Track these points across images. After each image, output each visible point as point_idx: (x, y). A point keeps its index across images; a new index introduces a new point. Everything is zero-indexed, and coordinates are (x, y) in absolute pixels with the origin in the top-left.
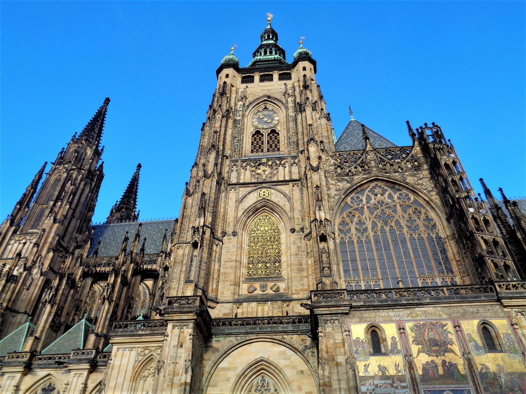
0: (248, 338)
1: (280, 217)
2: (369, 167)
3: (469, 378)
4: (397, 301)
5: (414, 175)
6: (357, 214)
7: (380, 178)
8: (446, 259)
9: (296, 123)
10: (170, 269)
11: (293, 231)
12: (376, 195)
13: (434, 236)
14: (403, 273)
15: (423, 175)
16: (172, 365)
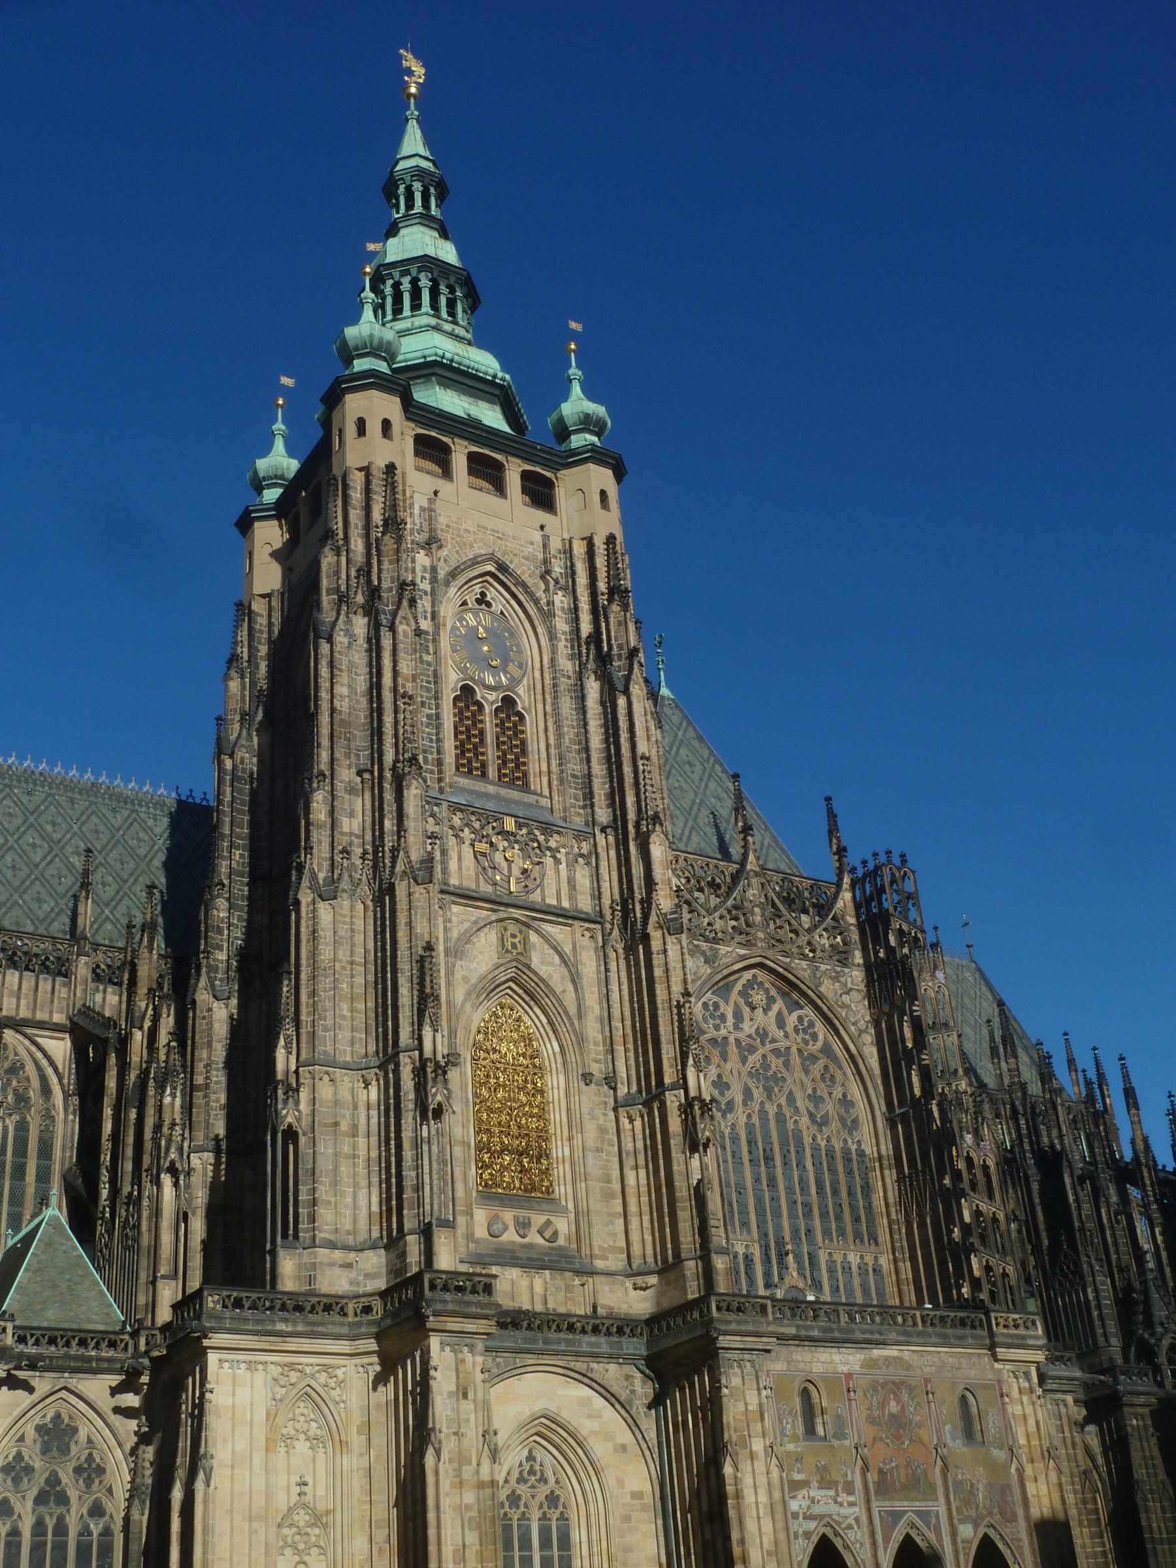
0: (519, 1363)
1: (550, 1022)
2: (748, 925)
3: (940, 1491)
4: (848, 1331)
5: (835, 979)
6: (715, 1053)
7: (768, 962)
8: (869, 1207)
9: (582, 710)
10: (302, 1140)
11: (587, 1078)
12: (753, 1008)
13: (854, 1147)
14: (795, 1232)
15: (852, 983)
16: (453, 1438)
